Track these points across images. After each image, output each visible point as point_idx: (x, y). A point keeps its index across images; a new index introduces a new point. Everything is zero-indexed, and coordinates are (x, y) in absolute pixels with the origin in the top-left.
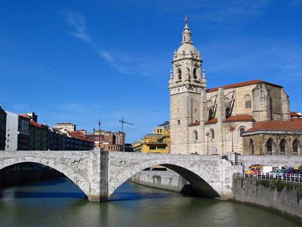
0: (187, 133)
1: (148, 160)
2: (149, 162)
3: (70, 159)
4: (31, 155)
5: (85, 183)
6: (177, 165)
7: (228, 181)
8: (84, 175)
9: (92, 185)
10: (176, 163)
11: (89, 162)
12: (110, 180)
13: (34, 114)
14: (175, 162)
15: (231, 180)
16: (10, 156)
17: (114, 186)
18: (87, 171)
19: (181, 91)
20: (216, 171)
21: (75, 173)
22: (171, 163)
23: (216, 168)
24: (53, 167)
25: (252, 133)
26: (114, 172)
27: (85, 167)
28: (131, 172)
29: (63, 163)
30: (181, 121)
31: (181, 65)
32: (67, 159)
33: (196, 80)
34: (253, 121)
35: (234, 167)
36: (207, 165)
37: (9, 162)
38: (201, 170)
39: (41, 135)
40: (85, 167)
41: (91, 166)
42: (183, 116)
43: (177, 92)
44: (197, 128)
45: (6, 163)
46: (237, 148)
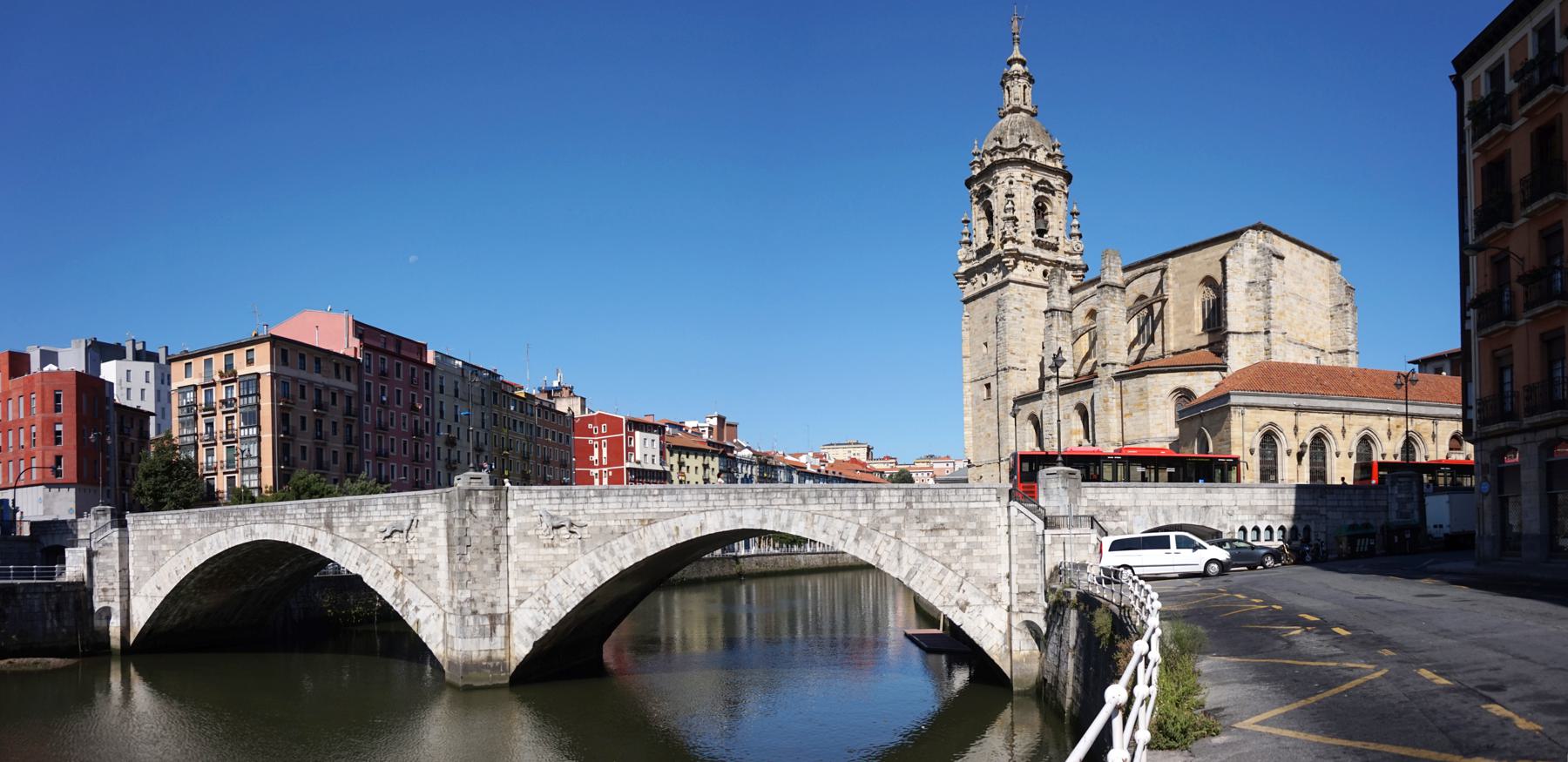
1: (672, 515)
2: (672, 523)
8: (426, 583)
10: (789, 525)
12: (520, 602)
13: (721, 420)
14: (784, 520)
17: (532, 624)
20: (983, 560)
23: (979, 546)
26: (530, 571)
27: (430, 551)
29: (356, 542)
32: (369, 524)
38: (910, 556)
40: (430, 551)
45: (208, 546)
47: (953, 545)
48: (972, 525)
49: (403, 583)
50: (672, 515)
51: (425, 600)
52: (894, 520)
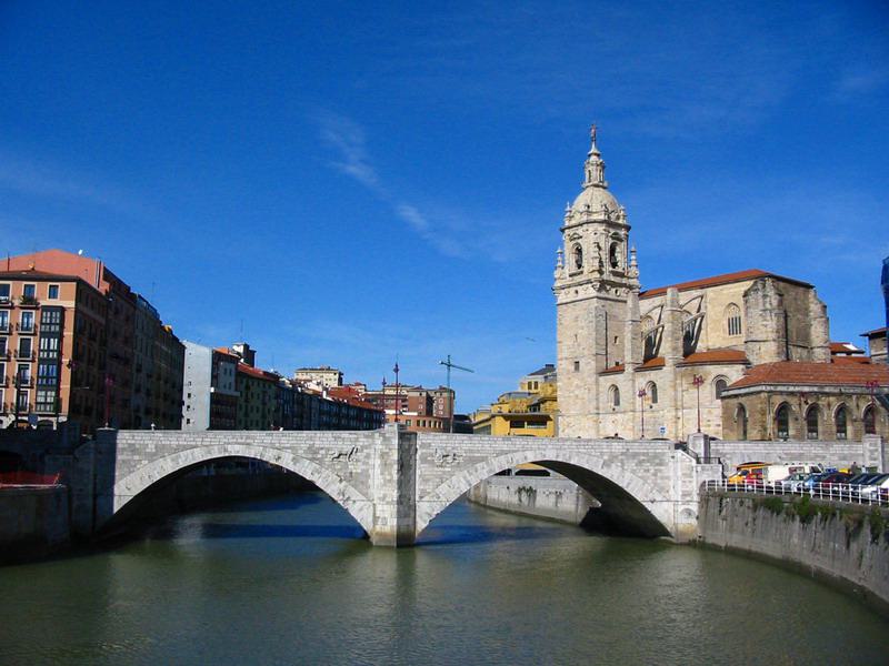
0: (594, 392)
3: (328, 449)
4: (240, 441)
6: (572, 462)
7: (688, 498)
8: (361, 486)
9: (379, 508)
10: (570, 457)
12: (421, 497)
13: (246, 347)
15: (696, 498)
16: (194, 443)
19: (580, 297)
20: (662, 478)
21: (341, 481)
22: (560, 460)
23: (660, 471)
24: (291, 468)
25: (743, 391)
26: (428, 480)
27: (364, 467)
28: (469, 478)
29: (312, 460)
33: (617, 269)
34: (746, 363)
35: (703, 469)
38: (628, 475)
39: (264, 396)
40: (364, 467)
41: (377, 466)
42: (586, 352)
43: (572, 297)
44: (618, 379)
47: (648, 471)
48: (657, 461)
49: (346, 486)
50: (509, 452)
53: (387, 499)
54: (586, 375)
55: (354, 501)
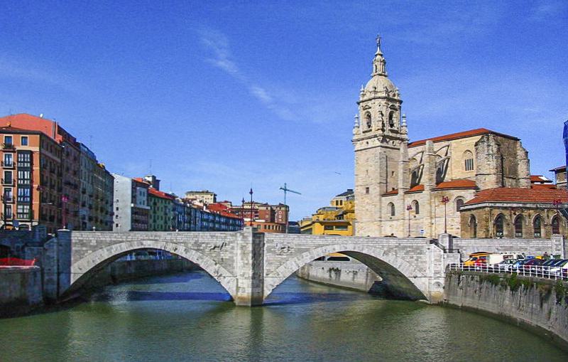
0: (378, 207)
3: (208, 244)
5: (229, 278)
6: (364, 252)
7: (438, 275)
9: (240, 281)
11: (236, 248)
12: (267, 275)
13: (154, 177)
15: (443, 275)
16: (121, 240)
17: (272, 283)
18: (233, 261)
20: (422, 262)
21: (216, 264)
26: (271, 263)
27: (230, 255)
29: (198, 250)
30: (370, 189)
31: (370, 108)
32: (203, 243)
33: (393, 128)
34: (476, 188)
36: (407, 253)
37: (119, 248)
38: (400, 260)
40: (230, 255)
42: (373, 181)
44: (394, 199)
46: (452, 229)
47: (412, 257)
48: (418, 251)
50: (324, 245)
51: (229, 274)
52: (395, 249)
53: (245, 276)
54: (373, 196)
55: (224, 277)
